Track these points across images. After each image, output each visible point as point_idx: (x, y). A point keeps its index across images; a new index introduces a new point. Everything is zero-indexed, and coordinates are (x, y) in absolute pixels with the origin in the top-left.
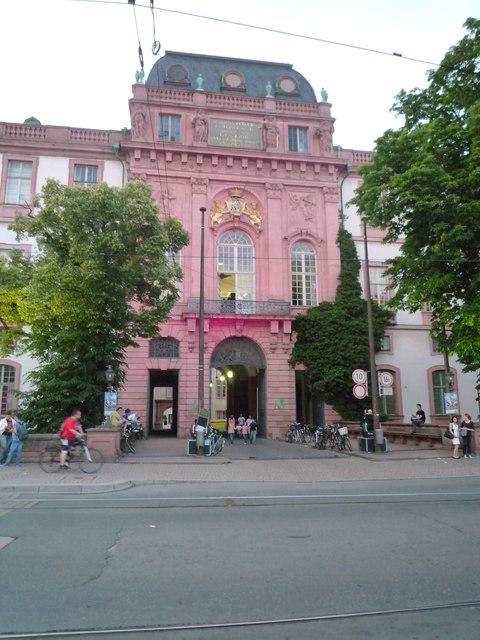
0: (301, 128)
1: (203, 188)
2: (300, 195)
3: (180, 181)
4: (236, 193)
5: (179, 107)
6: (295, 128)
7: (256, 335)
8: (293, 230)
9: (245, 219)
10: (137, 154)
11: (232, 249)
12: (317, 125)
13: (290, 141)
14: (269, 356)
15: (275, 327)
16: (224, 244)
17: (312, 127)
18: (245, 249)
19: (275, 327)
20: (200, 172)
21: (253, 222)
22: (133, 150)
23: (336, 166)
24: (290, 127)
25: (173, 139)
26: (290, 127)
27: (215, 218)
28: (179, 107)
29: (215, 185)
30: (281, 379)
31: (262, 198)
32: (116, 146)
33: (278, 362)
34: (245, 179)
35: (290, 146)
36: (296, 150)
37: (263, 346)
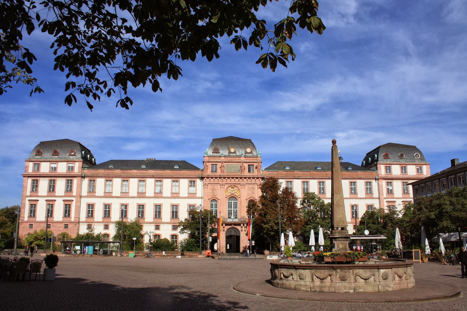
0: (252, 165)
1: (223, 186)
2: (251, 186)
3: (217, 184)
4: (233, 186)
5: (217, 162)
6: (250, 165)
7: (239, 228)
8: (249, 197)
9: (235, 194)
10: (206, 178)
11: (232, 202)
12: (257, 164)
13: (249, 169)
14: (241, 232)
15: (242, 225)
16: (229, 201)
17: (255, 164)
18: (235, 202)
19: (242, 225)
20: (223, 182)
21: (237, 195)
22: (204, 178)
23: (261, 178)
24: (249, 165)
25: (215, 171)
26: (249, 165)
27: (227, 194)
28: (217, 162)
29: (227, 185)
30: (244, 238)
31: (240, 188)
32: (200, 176)
33: (243, 234)
34: (235, 183)
35: (249, 170)
36: (250, 172)
37: (239, 230)
